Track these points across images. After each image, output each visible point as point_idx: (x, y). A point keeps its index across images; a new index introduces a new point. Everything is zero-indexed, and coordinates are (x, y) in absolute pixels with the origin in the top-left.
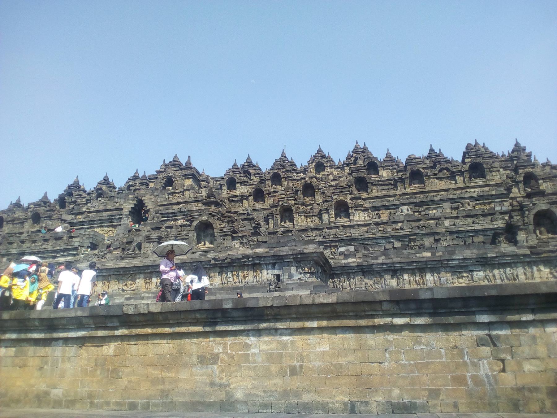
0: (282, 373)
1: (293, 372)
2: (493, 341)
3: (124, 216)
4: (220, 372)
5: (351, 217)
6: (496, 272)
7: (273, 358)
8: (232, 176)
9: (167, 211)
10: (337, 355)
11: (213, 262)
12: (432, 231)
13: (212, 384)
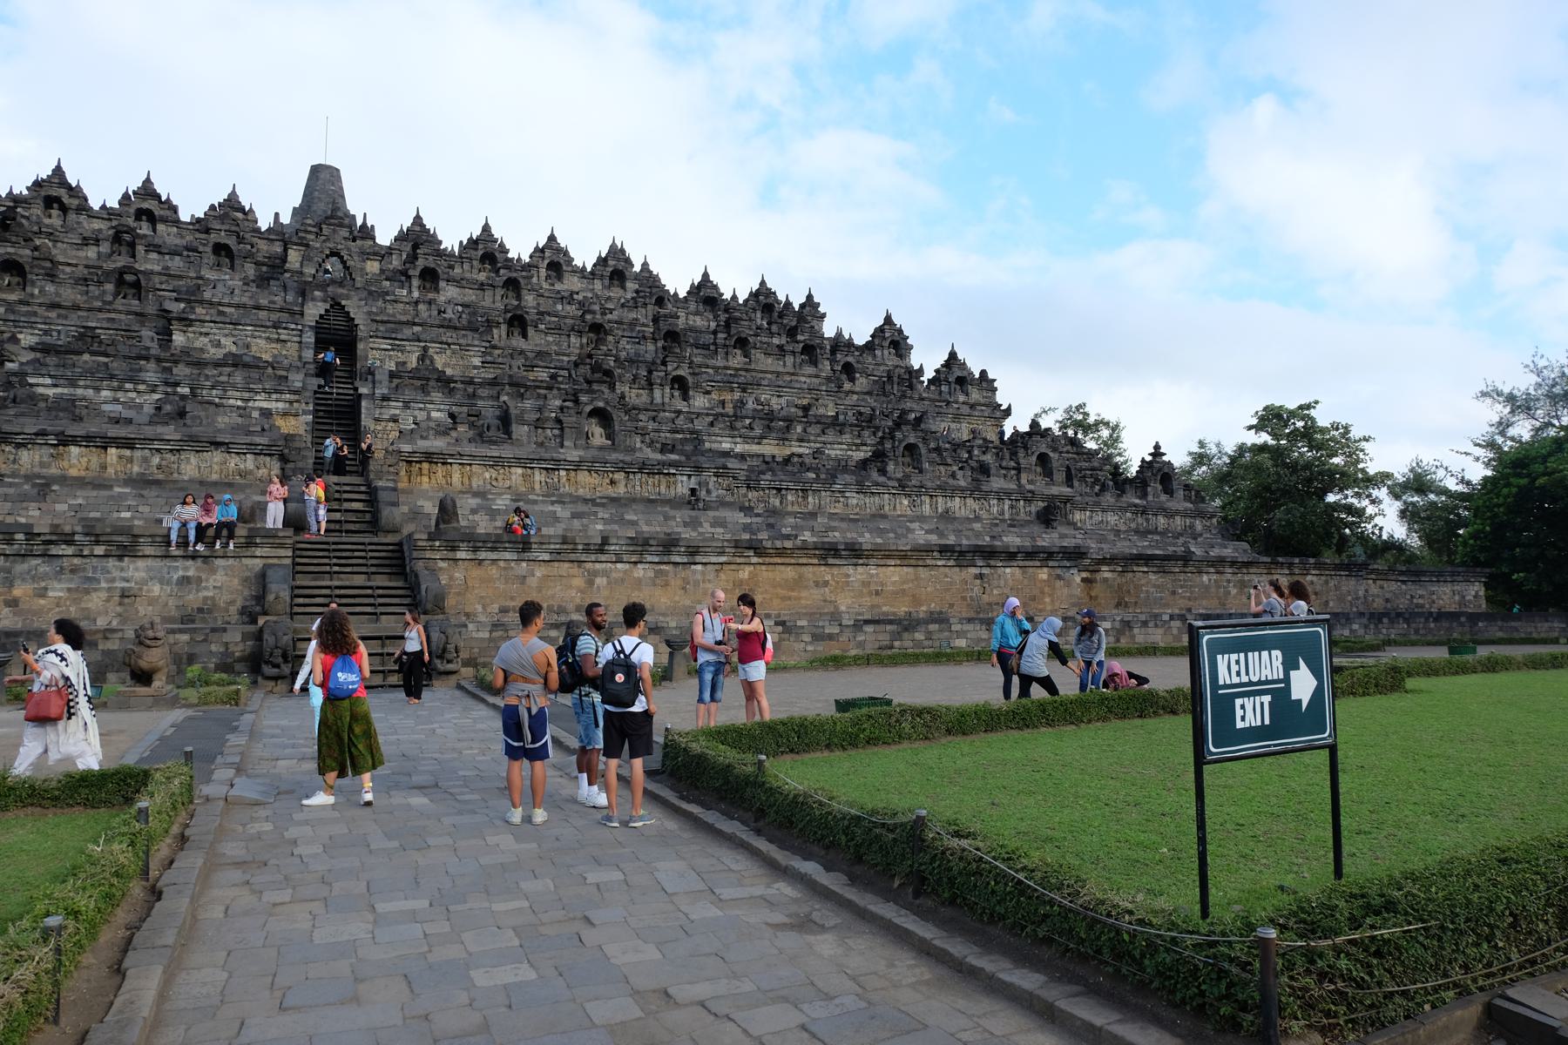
0: (870, 594)
1: (877, 593)
2: (981, 576)
3: (307, 329)
4: (831, 592)
5: (691, 402)
6: (867, 500)
7: (865, 584)
8: (432, 266)
9: (393, 336)
10: (904, 583)
11: (621, 465)
12: (784, 436)
13: (825, 601)
